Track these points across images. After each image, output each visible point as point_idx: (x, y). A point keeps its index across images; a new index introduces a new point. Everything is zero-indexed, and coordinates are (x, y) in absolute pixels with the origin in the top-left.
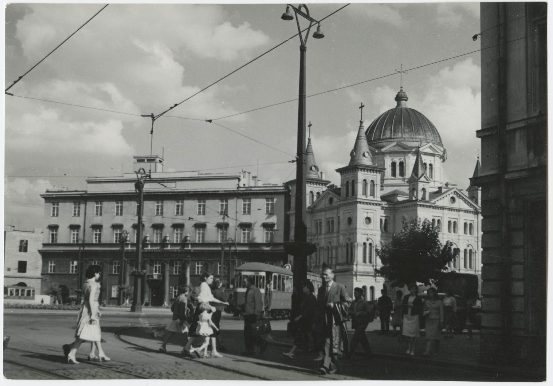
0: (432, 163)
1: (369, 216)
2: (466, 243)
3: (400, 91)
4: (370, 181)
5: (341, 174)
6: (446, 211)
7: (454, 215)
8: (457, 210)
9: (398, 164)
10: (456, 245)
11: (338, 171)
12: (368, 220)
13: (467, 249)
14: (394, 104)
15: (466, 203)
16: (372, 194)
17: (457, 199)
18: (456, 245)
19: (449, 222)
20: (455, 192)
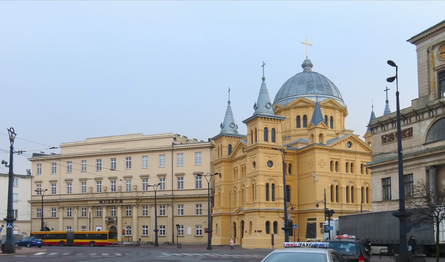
0: (333, 115)
1: (270, 160)
2: (363, 181)
4: (271, 129)
5: (247, 125)
6: (343, 154)
7: (351, 158)
8: (353, 153)
9: (302, 117)
10: (353, 183)
11: (243, 122)
12: (270, 164)
13: (364, 186)
15: (362, 147)
16: (274, 140)
17: (354, 144)
18: (353, 183)
19: (347, 163)
20: (351, 137)
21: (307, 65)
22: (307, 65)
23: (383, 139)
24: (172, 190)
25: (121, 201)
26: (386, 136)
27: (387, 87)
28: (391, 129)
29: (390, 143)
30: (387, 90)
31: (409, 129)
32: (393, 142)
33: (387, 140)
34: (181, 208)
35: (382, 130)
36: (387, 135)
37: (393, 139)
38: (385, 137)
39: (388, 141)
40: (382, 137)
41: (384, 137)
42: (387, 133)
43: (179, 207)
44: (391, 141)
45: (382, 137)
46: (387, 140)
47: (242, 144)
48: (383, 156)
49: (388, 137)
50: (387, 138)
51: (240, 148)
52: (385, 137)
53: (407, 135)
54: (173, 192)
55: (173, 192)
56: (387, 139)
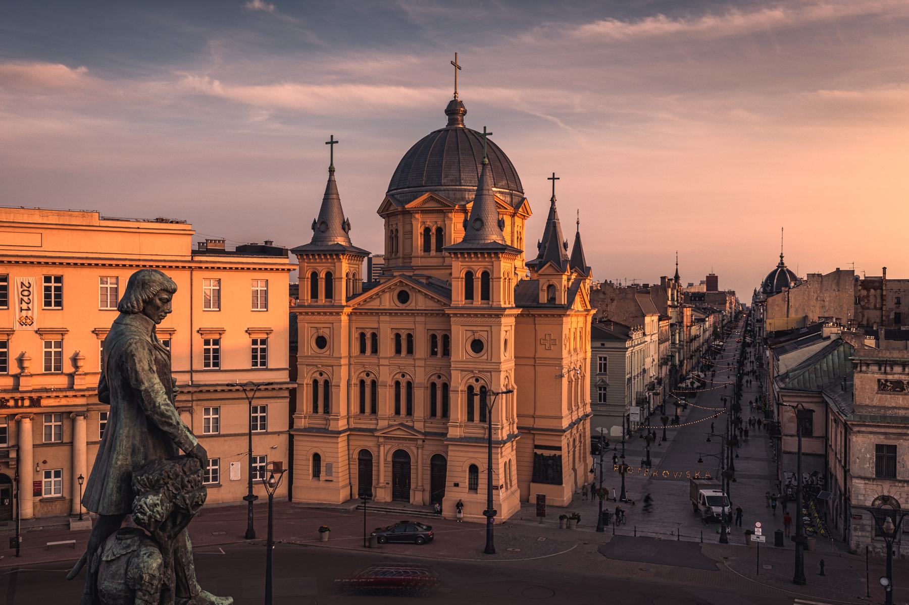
21: (454, 109)
22: (454, 109)
23: (879, 384)
24: (191, 372)
25: (35, 403)
26: (886, 381)
27: (554, 174)
28: (900, 374)
29: (896, 393)
30: (553, 179)
32: (900, 393)
33: (889, 388)
34: (211, 416)
35: (880, 369)
37: (903, 389)
38: (884, 382)
39: (890, 389)
40: (879, 381)
42: (890, 377)
43: (207, 411)
44: (897, 391)
45: (879, 381)
46: (889, 388)
47: (401, 282)
48: (880, 410)
49: (891, 384)
50: (888, 384)
51: (394, 290)
52: (884, 382)
54: (194, 374)
55: (194, 374)
56: (888, 386)
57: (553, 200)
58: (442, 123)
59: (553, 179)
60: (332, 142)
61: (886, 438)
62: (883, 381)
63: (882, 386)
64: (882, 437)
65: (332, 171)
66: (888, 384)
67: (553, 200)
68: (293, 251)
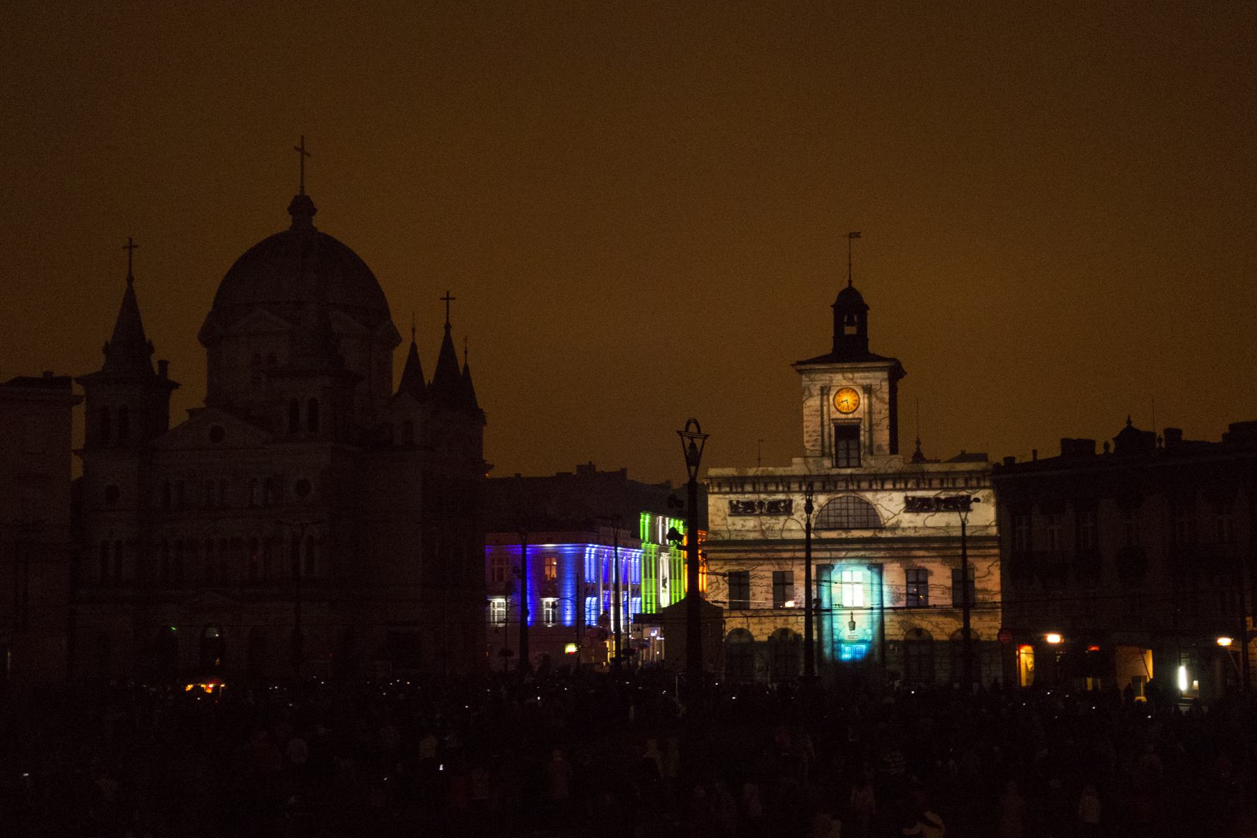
3: (298, 193)
14: (284, 223)
21: (302, 207)
22: (302, 207)
26: (738, 502)
30: (448, 299)
31: (784, 501)
33: (741, 510)
36: (742, 502)
37: (754, 510)
41: (734, 502)
45: (731, 502)
50: (740, 506)
53: (782, 510)
56: (740, 508)
57: (448, 327)
58: (284, 223)
59: (448, 299)
60: (131, 247)
61: (738, 565)
62: (734, 502)
63: (735, 510)
64: (734, 563)
65: (130, 279)
66: (740, 506)
67: (448, 327)
68: (80, 380)
